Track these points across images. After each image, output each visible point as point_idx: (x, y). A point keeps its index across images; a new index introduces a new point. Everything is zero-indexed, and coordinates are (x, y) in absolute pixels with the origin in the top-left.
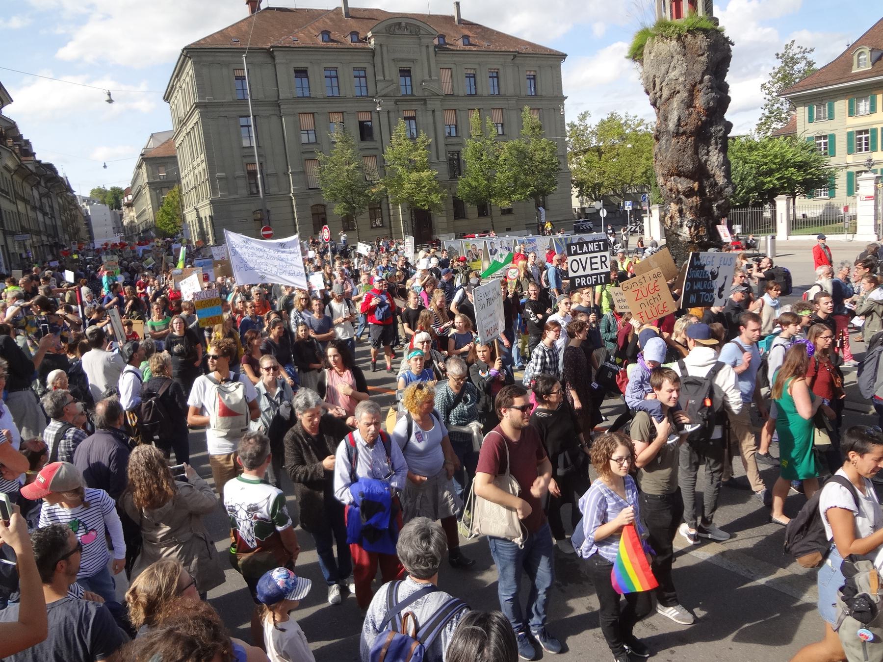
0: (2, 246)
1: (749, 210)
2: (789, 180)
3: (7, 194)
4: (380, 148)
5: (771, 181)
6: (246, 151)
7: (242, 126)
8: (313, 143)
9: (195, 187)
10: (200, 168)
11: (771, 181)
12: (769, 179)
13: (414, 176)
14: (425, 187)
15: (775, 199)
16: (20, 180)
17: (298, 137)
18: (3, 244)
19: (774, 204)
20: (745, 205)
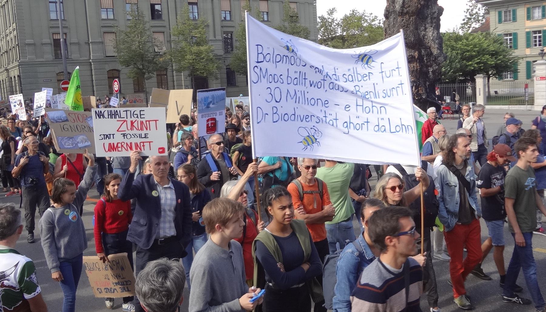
1: (456, 85)
2: (485, 63)
4: (168, 26)
5: (471, 65)
7: (50, 2)
9: (7, 52)
11: (473, 64)
12: (470, 63)
13: (195, 49)
14: (203, 58)
15: (475, 77)
19: (473, 81)
20: (453, 81)
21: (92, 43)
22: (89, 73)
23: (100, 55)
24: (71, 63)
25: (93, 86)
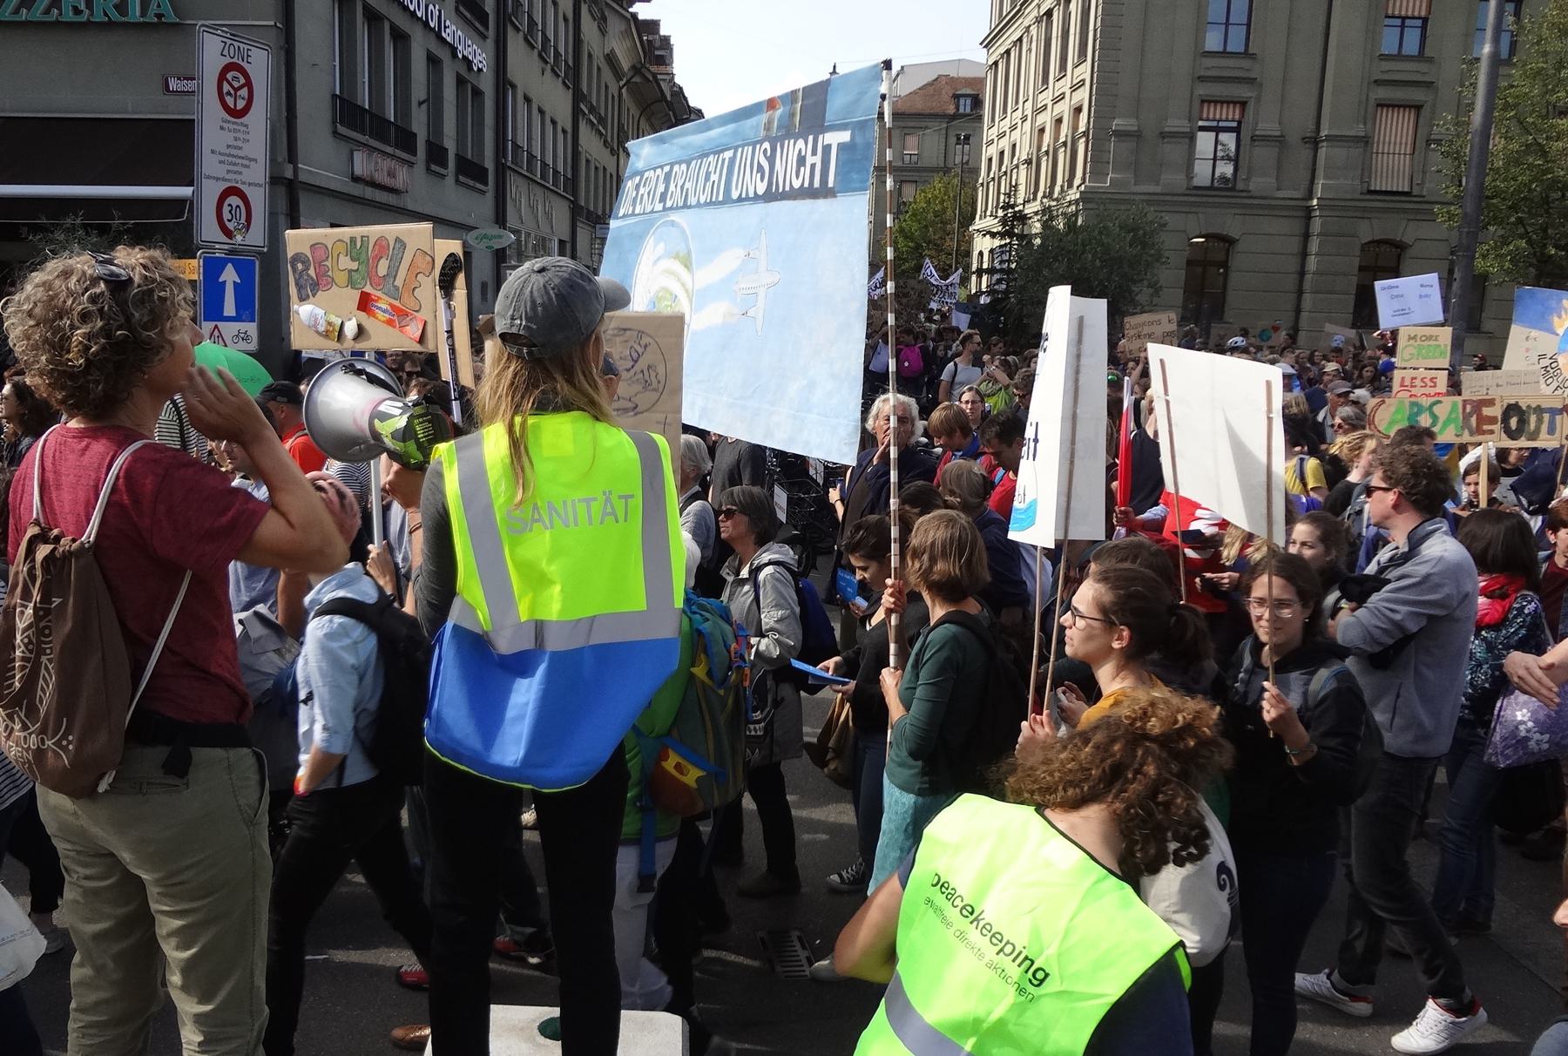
0: (561, 242)
3: (602, 121)
6: (1209, 62)
8: (1410, 58)
9: (1028, 162)
10: (1064, 108)
16: (634, 111)
17: (1372, 35)
18: (566, 237)
21: (1329, 138)
22: (1294, 244)
23: (1348, 185)
24: (1245, 206)
25: (1300, 292)
